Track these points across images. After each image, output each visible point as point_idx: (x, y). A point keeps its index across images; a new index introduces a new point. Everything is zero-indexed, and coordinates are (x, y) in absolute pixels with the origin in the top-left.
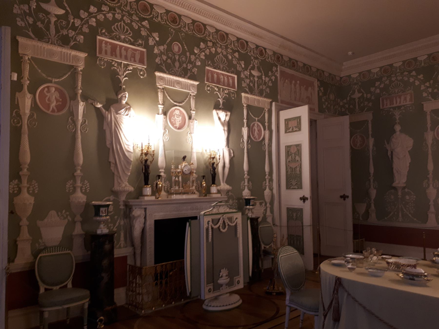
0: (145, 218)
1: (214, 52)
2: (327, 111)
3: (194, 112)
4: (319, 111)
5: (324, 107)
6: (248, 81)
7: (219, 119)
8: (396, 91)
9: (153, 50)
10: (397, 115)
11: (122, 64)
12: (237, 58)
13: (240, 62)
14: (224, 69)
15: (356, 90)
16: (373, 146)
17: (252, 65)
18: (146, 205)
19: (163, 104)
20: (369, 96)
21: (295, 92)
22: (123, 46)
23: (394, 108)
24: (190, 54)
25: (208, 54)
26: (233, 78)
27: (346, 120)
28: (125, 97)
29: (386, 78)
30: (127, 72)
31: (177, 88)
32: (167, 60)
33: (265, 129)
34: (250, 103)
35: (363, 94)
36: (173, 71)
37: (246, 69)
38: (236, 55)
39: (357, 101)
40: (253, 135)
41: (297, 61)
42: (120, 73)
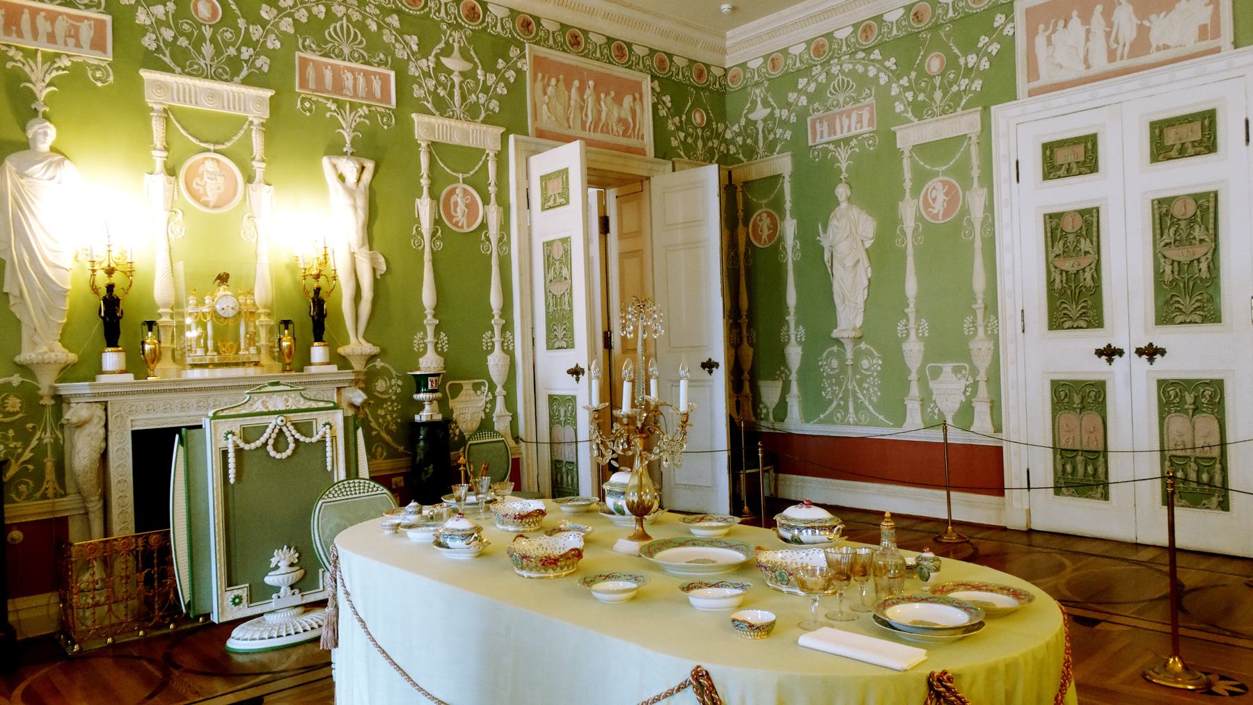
0: (106, 426)
1: (322, 16)
3: (264, 165)
5: (674, 143)
6: (431, 83)
7: (342, 178)
8: (841, 101)
9: (134, 17)
10: (844, 160)
11: (39, 54)
12: (395, 29)
13: (407, 37)
14: (356, 55)
15: (759, 100)
17: (442, 45)
18: (105, 394)
19: (166, 149)
20: (785, 113)
21: (582, 108)
22: (42, 10)
23: (837, 143)
24: (248, 23)
25: (304, 20)
26: (385, 80)
28: (45, 134)
29: (819, 67)
30: (55, 74)
31: (207, 106)
32: (175, 38)
33: (486, 202)
34: (437, 138)
35: (773, 109)
36: (196, 67)
37: (424, 52)
38: (394, 20)
40: (450, 217)
41: (585, 32)
42: (33, 78)
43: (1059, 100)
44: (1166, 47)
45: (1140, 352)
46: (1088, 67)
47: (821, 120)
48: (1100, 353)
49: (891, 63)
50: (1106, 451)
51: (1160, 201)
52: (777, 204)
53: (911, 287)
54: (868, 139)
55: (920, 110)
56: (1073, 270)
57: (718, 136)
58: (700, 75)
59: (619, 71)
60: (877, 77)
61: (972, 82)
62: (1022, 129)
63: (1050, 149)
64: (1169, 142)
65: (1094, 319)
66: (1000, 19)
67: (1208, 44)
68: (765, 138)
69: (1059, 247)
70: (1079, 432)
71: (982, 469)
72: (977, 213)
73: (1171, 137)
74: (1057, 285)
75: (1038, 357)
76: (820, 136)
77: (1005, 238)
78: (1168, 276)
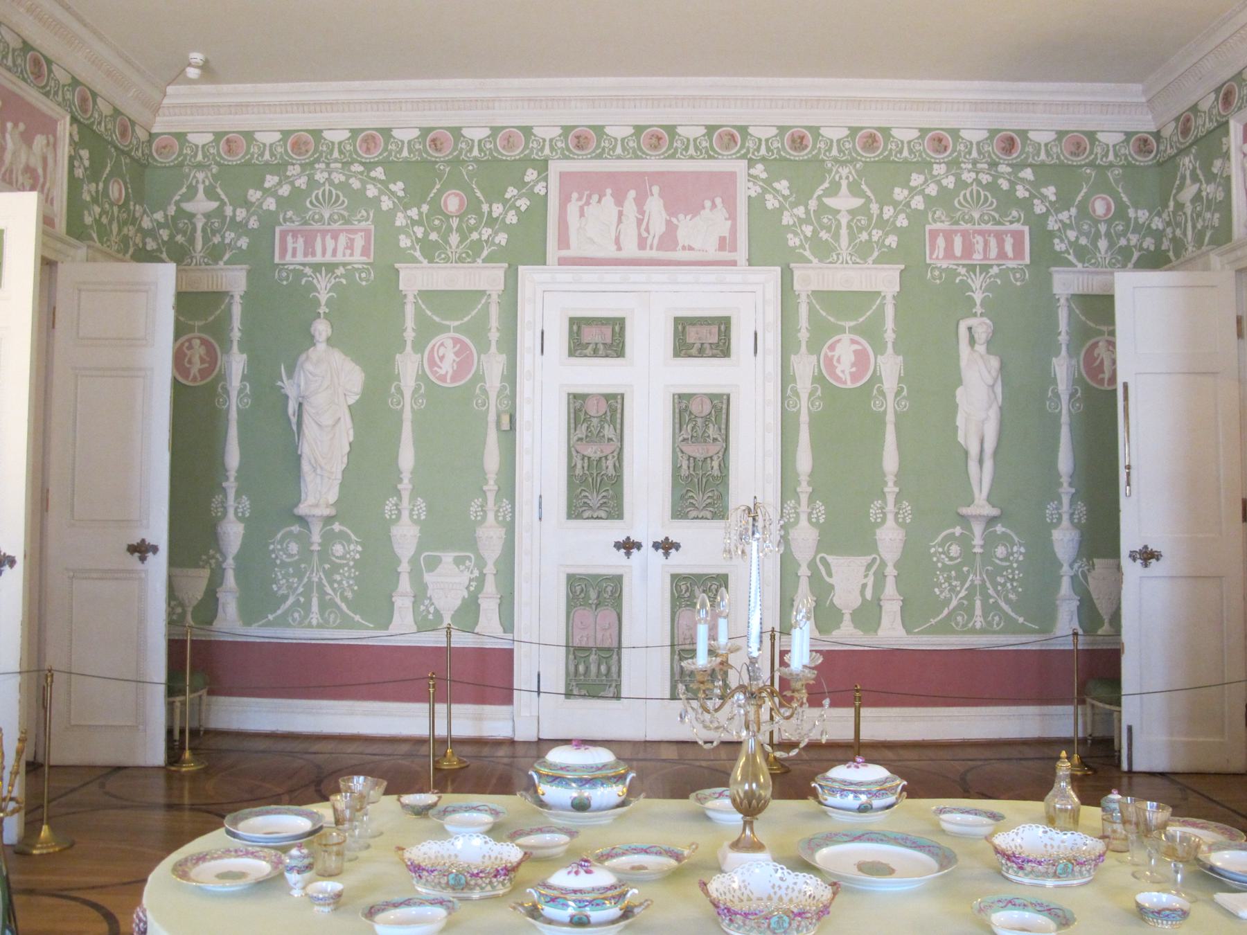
2: (95, 236)
4: (69, 233)
5: (88, 220)
8: (326, 216)
10: (324, 289)
15: (201, 187)
16: (244, 378)
20: (241, 214)
23: (317, 267)
27: (164, 278)
29: (298, 169)
35: (223, 204)
39: (199, 226)
43: (589, 275)
44: (691, 248)
45: (656, 546)
46: (619, 249)
47: (295, 234)
48: (618, 546)
49: (398, 187)
50: (620, 647)
51: (681, 396)
52: (219, 330)
53: (407, 458)
54: (360, 271)
55: (431, 251)
56: (595, 456)
57: (134, 221)
58: (123, 134)
59: (32, 95)
60: (377, 200)
61: (496, 234)
62: (550, 298)
63: (577, 325)
64: (690, 340)
65: (614, 509)
66: (531, 175)
67: (726, 256)
68: (206, 240)
69: (582, 431)
70: (594, 631)
71: (489, 676)
72: (494, 381)
73: (692, 335)
74: (578, 471)
75: (556, 546)
76: (293, 254)
77: (524, 414)
78: (684, 471)
